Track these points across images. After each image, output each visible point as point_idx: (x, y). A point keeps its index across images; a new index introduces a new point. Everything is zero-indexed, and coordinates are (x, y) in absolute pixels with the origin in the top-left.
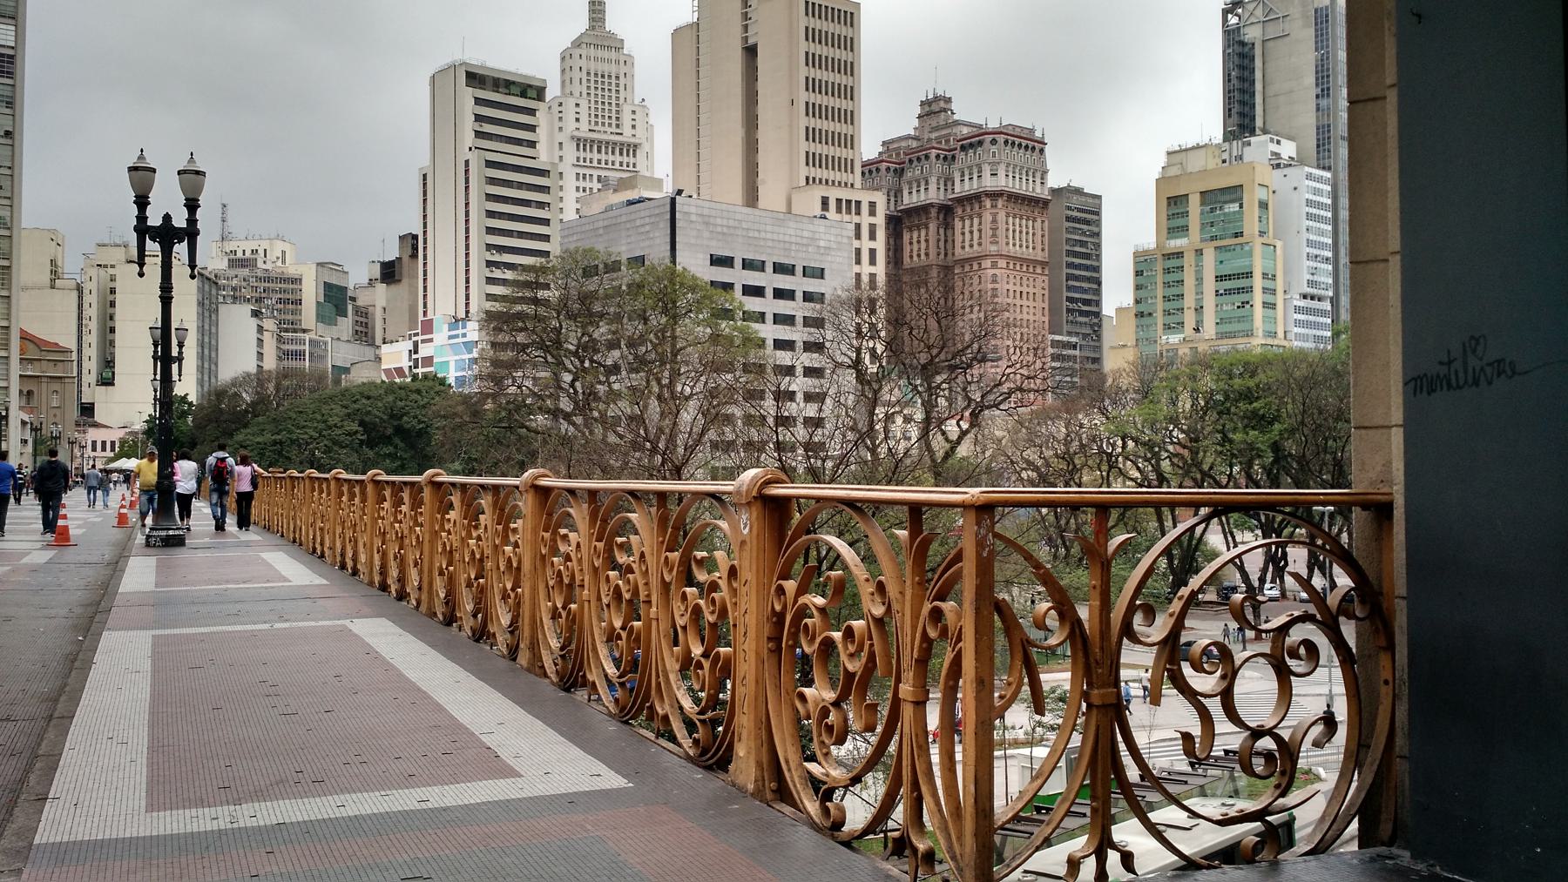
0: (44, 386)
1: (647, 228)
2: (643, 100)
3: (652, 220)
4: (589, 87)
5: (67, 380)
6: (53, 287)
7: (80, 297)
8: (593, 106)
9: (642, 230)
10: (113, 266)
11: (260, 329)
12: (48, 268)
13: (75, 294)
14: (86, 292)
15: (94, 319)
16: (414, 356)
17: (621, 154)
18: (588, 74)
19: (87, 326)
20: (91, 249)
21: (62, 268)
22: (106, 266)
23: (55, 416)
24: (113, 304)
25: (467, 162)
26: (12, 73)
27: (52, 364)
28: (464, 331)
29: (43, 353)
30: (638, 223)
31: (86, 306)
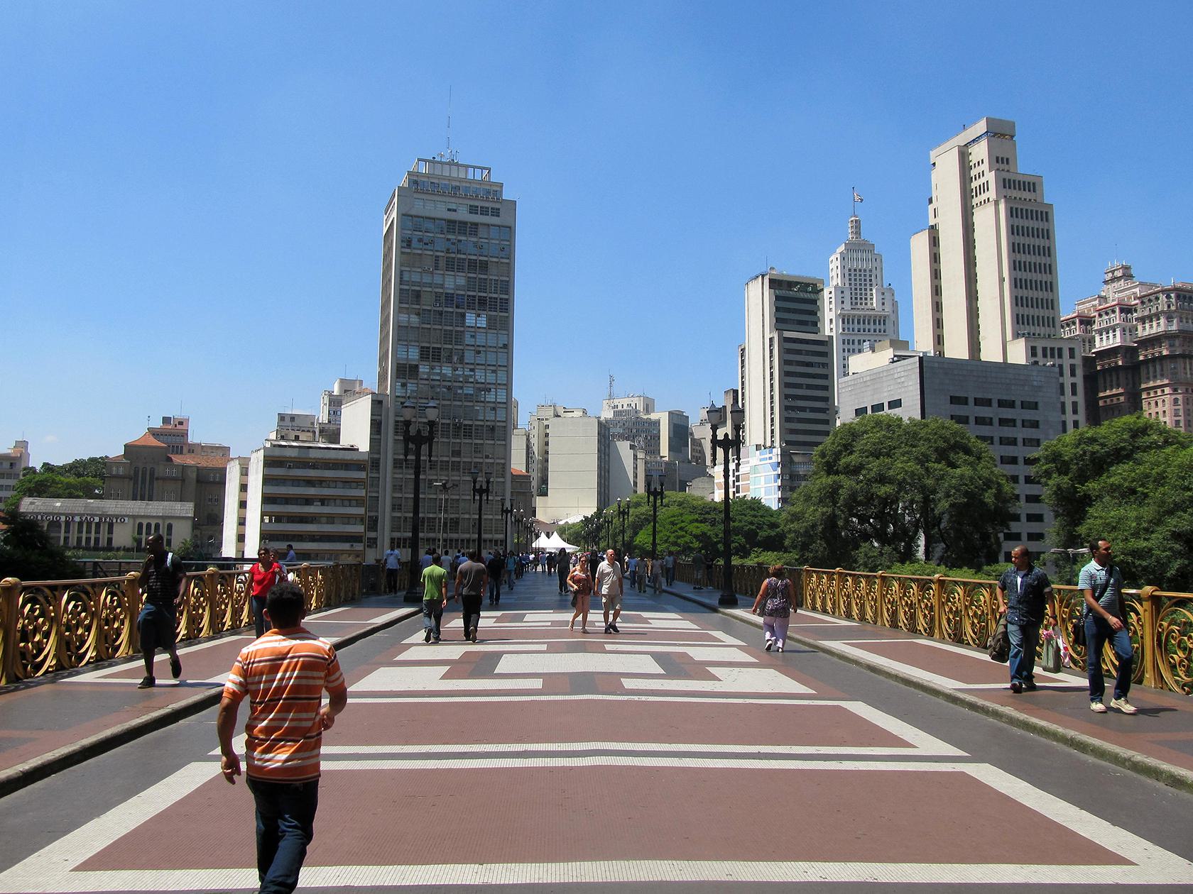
1: (903, 379)
2: (890, 285)
3: (906, 374)
4: (850, 280)
8: (853, 292)
9: (899, 381)
10: (546, 419)
11: (635, 458)
16: (736, 474)
17: (875, 323)
18: (850, 270)
20: (534, 410)
22: (543, 419)
24: (547, 444)
25: (771, 340)
26: (507, 309)
28: (771, 455)
30: (896, 376)
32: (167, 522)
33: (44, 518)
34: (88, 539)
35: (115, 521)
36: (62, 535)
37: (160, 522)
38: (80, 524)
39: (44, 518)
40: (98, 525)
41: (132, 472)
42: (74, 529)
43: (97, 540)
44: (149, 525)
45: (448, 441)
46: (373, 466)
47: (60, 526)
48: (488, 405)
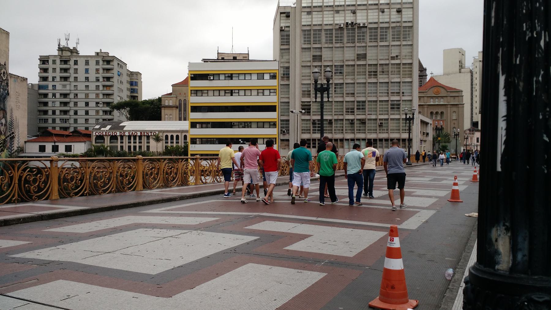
0: (449, 109)
5: (460, 106)
6: (460, 72)
7: (472, 76)
12: (458, 64)
13: (469, 74)
14: (474, 73)
15: (478, 84)
19: (475, 88)
21: (465, 65)
23: (454, 124)
27: (452, 98)
29: (448, 93)
31: (474, 79)
32: (184, 134)
33: (107, 134)
34: (135, 147)
35: (150, 134)
36: (119, 145)
37: (179, 134)
38: (129, 137)
39: (107, 134)
40: (140, 137)
41: (178, 104)
42: (126, 140)
43: (140, 147)
44: (172, 137)
45: (353, 45)
46: (284, 74)
47: (117, 139)
48: (393, 6)
